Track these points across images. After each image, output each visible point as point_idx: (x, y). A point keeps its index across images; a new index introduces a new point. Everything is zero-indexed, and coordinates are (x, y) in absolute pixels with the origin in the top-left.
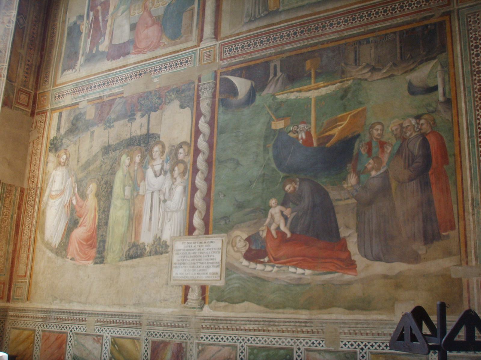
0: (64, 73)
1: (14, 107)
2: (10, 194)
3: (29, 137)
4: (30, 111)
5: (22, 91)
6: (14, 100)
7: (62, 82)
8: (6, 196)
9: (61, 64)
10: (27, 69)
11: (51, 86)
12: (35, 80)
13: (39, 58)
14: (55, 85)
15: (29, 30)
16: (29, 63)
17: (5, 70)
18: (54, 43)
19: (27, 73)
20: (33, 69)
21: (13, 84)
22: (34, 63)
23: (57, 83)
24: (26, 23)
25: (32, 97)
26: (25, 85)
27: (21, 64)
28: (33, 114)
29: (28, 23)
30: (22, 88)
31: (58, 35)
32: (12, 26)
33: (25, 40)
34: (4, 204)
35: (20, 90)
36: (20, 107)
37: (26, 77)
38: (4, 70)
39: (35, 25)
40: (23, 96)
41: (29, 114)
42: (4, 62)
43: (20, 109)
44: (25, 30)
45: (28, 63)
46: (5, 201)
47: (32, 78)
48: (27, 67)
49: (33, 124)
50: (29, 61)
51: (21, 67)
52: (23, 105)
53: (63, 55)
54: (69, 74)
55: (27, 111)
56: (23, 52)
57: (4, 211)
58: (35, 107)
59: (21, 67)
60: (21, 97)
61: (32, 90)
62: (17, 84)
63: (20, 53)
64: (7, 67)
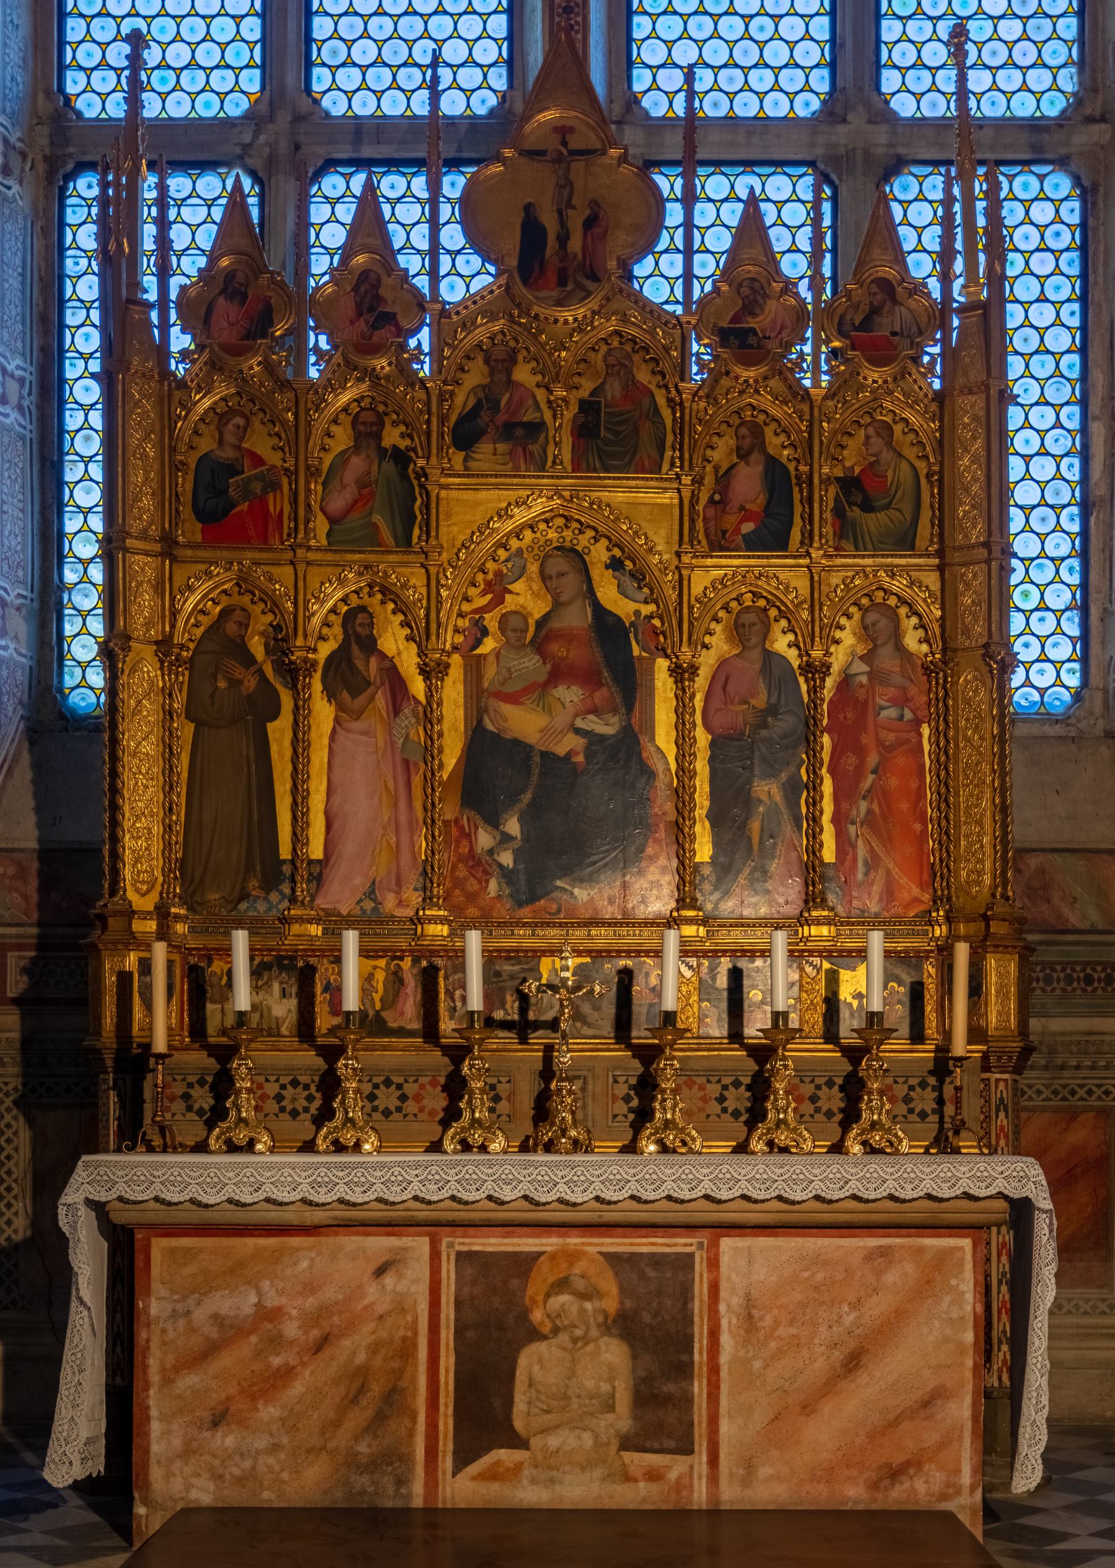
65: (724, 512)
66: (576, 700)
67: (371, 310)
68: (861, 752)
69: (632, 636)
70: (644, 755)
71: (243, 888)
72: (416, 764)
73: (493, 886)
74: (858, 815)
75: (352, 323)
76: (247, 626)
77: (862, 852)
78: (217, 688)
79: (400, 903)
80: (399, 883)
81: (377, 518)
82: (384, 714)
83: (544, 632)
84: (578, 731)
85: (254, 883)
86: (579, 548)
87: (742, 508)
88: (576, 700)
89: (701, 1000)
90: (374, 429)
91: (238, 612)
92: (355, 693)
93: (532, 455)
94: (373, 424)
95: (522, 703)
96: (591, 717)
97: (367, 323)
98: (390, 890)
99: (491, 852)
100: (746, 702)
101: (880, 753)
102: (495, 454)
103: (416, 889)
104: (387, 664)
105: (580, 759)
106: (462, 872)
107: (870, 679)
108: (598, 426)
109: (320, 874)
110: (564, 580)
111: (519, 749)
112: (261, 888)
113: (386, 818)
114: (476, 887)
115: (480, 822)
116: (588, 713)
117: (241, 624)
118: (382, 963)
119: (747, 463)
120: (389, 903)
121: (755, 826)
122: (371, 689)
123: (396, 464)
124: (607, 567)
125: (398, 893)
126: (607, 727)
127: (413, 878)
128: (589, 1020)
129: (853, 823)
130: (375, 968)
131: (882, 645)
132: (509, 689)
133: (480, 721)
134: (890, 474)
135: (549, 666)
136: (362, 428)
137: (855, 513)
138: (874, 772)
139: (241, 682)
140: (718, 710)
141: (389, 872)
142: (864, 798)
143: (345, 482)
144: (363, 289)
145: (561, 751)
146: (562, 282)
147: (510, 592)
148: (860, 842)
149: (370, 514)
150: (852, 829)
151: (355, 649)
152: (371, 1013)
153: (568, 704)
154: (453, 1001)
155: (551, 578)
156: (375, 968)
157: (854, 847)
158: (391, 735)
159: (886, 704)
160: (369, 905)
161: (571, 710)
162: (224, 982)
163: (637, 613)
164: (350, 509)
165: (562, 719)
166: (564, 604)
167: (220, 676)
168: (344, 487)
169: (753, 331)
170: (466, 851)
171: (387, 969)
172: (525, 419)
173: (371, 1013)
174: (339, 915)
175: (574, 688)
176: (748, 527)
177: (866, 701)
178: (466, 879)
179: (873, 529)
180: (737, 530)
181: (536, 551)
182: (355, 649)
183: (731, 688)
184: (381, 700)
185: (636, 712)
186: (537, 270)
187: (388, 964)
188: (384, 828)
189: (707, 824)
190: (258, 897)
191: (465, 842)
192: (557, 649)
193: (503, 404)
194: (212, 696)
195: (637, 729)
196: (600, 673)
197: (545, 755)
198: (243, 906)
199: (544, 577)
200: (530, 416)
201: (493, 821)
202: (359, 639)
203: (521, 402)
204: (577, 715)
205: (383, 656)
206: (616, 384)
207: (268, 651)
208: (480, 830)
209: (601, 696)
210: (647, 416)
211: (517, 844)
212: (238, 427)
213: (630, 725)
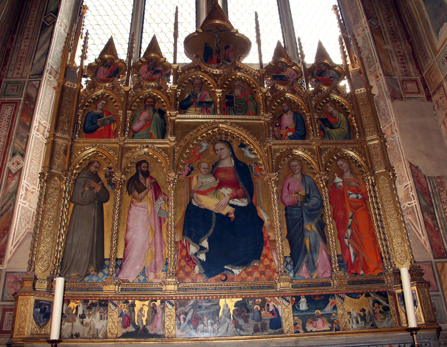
0: (440, 34)
1: (405, 98)
2: (442, 187)
3: (437, 121)
4: (424, 96)
5: (405, 81)
6: (402, 92)
7: (442, 43)
8: (439, 190)
9: (432, 30)
10: (401, 59)
11: (433, 58)
12: (415, 67)
13: (409, 46)
14: (435, 52)
15: (385, 27)
16: (401, 54)
17: (379, 69)
18: (416, 21)
19: (403, 63)
20: (408, 57)
21: (394, 77)
22: (406, 52)
23: (438, 49)
24: (380, 23)
25: (420, 83)
26: (406, 73)
27: (392, 57)
28: (429, 98)
29: (381, 21)
30: (404, 78)
31: (416, 13)
32: (368, 31)
33: (386, 36)
34: (441, 199)
35: (402, 81)
36: (411, 96)
37: (404, 67)
38: (378, 70)
39: (389, 21)
40: (409, 85)
41: (426, 99)
42: (375, 64)
43: (413, 97)
44: (382, 29)
45: (399, 54)
46: (440, 196)
47: (410, 65)
48: (400, 58)
49: (434, 107)
50: (399, 52)
51: (393, 60)
52: (414, 93)
53: (429, 22)
54: (445, 28)
55: (421, 97)
56: (389, 47)
57: (444, 207)
58: (428, 90)
59: (393, 60)
60: (408, 87)
61: (416, 76)
62: (398, 75)
63: (387, 49)
64: (379, 65)
65: (280, 129)
67: (153, 69)
68: (345, 211)
70: (259, 214)
71: (88, 271)
72: (164, 219)
73: (197, 269)
74: (348, 235)
75: (146, 73)
76: (99, 168)
77: (351, 250)
78: (85, 190)
79: (156, 277)
80: (155, 269)
81: (151, 131)
82: (151, 199)
84: (232, 205)
85: (92, 268)
86: (228, 140)
87: (287, 128)
88: (229, 193)
89: (294, 316)
90: (152, 104)
91: (96, 163)
92: (139, 192)
93: (209, 111)
94: (151, 102)
95: (208, 195)
96: (236, 200)
97: (151, 73)
98: (151, 271)
99: (196, 254)
100: (297, 193)
101: (352, 211)
102: (196, 111)
103: (163, 271)
104: (153, 181)
105: (232, 216)
106: (183, 263)
107: (343, 184)
108: (233, 102)
109: (121, 265)
110: (222, 151)
111: (207, 212)
112: (95, 271)
113: (150, 241)
114: (189, 269)
115: (191, 242)
117: (96, 167)
118: (147, 303)
119: (287, 114)
120: (151, 276)
121: (307, 242)
122: (147, 190)
123: (159, 114)
125: (155, 272)
126: (242, 203)
127: (161, 266)
128: (243, 327)
129: (346, 238)
130: (144, 305)
131: (346, 172)
132: (202, 189)
133: (190, 202)
134: (337, 117)
135: (218, 181)
136: (147, 103)
137: (328, 129)
138: (351, 218)
139: (94, 188)
140: (287, 196)
141: (151, 263)
142: (349, 228)
143: (140, 119)
144: (150, 64)
145: (224, 213)
146: (218, 62)
148: (350, 245)
149: (149, 130)
150: (346, 241)
151: (141, 176)
152: (141, 327)
153: (226, 195)
154: (180, 320)
155: (217, 150)
156: (144, 305)
157: (349, 249)
158: (154, 207)
159: (351, 193)
160: (142, 278)
161: (228, 197)
162: (74, 312)
164: (141, 129)
165: (224, 201)
166: (223, 159)
167: (86, 186)
168: (140, 121)
169: (284, 76)
171: (149, 306)
172: (206, 101)
173: (141, 327)
174: (129, 282)
175: (228, 189)
176: (290, 134)
177: (343, 192)
178: (185, 266)
179: (335, 134)
180: (286, 135)
182: (141, 176)
183: (290, 188)
184: (150, 194)
185: (254, 198)
186: (210, 59)
187: (149, 303)
188: (150, 245)
189: (287, 240)
190: (93, 275)
191: (184, 251)
192: (222, 175)
193: (198, 96)
194: (82, 193)
195: (254, 204)
196: (238, 183)
197: (217, 214)
198: (86, 279)
199: (215, 150)
200: (209, 99)
201: (197, 241)
202: (142, 172)
203: (205, 96)
204: (230, 199)
205: (152, 178)
206: (238, 91)
207: (106, 177)
209: (240, 191)
210: (250, 100)
212: (103, 104)
213: (252, 202)
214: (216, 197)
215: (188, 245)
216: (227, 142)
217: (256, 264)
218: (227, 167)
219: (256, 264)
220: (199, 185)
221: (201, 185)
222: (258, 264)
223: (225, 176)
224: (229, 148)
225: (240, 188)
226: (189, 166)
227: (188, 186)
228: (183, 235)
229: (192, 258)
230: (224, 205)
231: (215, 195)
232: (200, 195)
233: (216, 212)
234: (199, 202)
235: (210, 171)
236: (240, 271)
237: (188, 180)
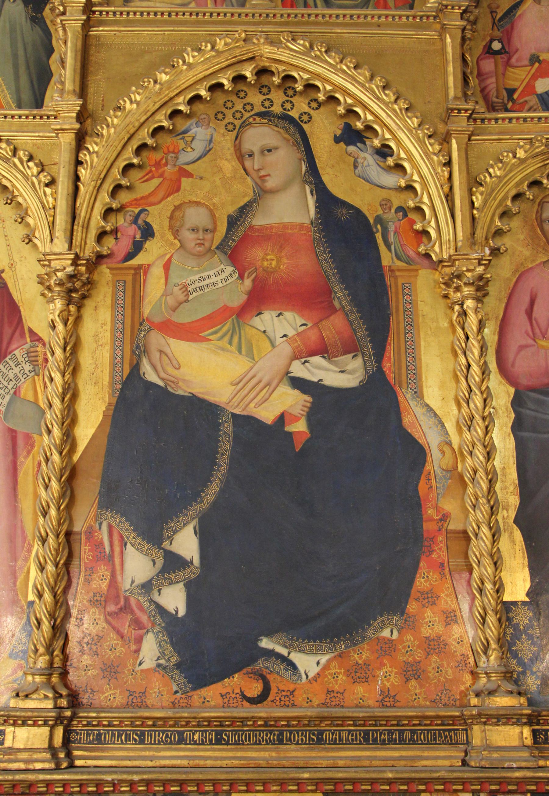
65: (508, 64)
66: (291, 333)
69: (379, 237)
70: (406, 421)
72: (28, 437)
83: (240, 232)
86: (294, 114)
87: (534, 59)
88: (291, 333)
95: (205, 340)
96: (317, 360)
110: (271, 158)
115: (130, 536)
116: (313, 353)
124: (337, 140)
133: (136, 368)
135: (248, 283)
140: (522, 347)
147: (189, 175)
153: (279, 341)
163: (386, 204)
166: (272, 192)
170: (104, 585)
175: (289, 315)
180: (530, 88)
181: (229, 118)
185: (390, 352)
189: (518, 535)
195: (391, 378)
196: (329, 292)
204: (296, 357)
208: (129, 545)
211: (193, 572)
213: (380, 369)
214: (240, 352)
215: (117, 549)
216: (291, 120)
217: (386, 633)
218: (285, 226)
219: (386, 633)
220: (171, 301)
221: (182, 297)
222: (395, 633)
223: (279, 261)
224: (296, 144)
225: (334, 311)
226: (135, 221)
227: (129, 301)
228: (101, 506)
229: (133, 602)
230: (269, 384)
231: (236, 340)
232: (172, 342)
233: (237, 411)
234: (170, 370)
235: (217, 240)
236: (324, 659)
237: (129, 279)
